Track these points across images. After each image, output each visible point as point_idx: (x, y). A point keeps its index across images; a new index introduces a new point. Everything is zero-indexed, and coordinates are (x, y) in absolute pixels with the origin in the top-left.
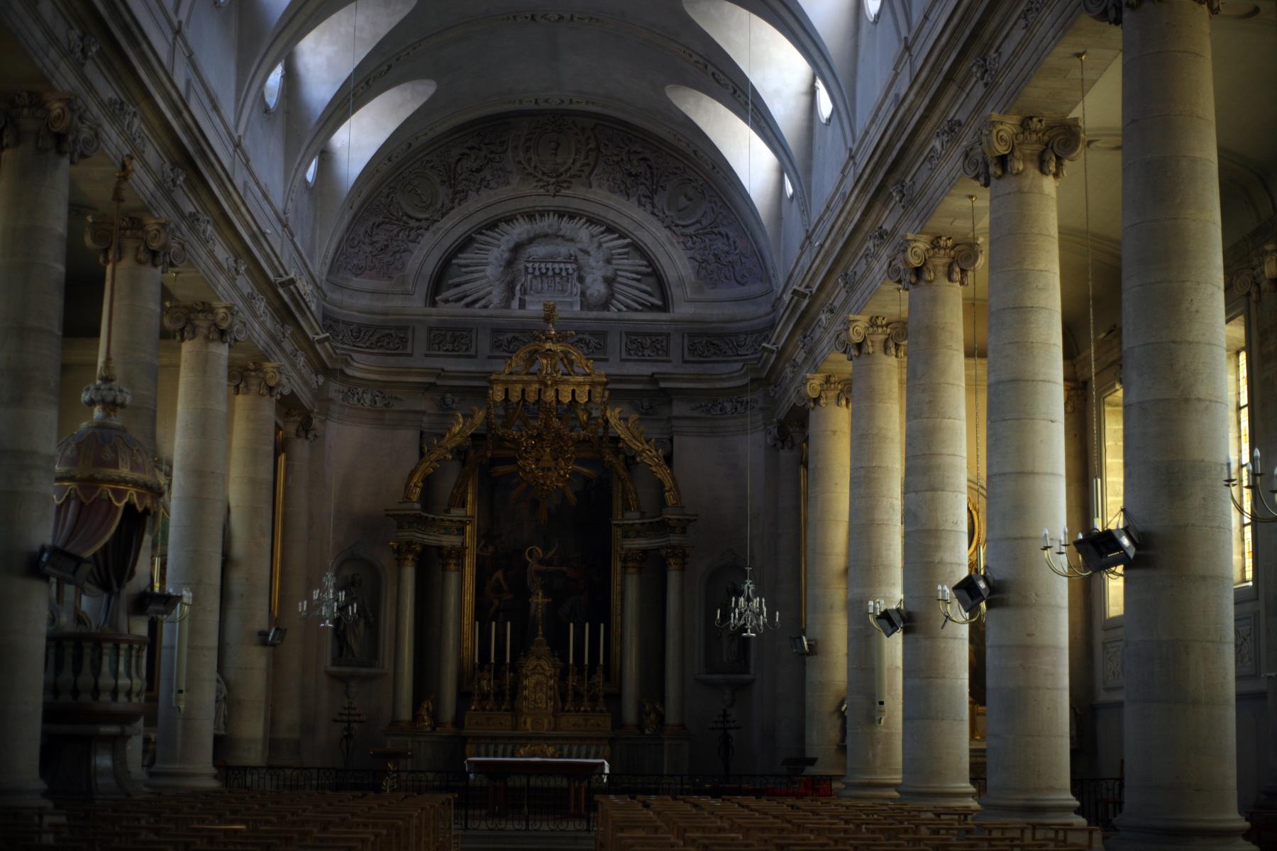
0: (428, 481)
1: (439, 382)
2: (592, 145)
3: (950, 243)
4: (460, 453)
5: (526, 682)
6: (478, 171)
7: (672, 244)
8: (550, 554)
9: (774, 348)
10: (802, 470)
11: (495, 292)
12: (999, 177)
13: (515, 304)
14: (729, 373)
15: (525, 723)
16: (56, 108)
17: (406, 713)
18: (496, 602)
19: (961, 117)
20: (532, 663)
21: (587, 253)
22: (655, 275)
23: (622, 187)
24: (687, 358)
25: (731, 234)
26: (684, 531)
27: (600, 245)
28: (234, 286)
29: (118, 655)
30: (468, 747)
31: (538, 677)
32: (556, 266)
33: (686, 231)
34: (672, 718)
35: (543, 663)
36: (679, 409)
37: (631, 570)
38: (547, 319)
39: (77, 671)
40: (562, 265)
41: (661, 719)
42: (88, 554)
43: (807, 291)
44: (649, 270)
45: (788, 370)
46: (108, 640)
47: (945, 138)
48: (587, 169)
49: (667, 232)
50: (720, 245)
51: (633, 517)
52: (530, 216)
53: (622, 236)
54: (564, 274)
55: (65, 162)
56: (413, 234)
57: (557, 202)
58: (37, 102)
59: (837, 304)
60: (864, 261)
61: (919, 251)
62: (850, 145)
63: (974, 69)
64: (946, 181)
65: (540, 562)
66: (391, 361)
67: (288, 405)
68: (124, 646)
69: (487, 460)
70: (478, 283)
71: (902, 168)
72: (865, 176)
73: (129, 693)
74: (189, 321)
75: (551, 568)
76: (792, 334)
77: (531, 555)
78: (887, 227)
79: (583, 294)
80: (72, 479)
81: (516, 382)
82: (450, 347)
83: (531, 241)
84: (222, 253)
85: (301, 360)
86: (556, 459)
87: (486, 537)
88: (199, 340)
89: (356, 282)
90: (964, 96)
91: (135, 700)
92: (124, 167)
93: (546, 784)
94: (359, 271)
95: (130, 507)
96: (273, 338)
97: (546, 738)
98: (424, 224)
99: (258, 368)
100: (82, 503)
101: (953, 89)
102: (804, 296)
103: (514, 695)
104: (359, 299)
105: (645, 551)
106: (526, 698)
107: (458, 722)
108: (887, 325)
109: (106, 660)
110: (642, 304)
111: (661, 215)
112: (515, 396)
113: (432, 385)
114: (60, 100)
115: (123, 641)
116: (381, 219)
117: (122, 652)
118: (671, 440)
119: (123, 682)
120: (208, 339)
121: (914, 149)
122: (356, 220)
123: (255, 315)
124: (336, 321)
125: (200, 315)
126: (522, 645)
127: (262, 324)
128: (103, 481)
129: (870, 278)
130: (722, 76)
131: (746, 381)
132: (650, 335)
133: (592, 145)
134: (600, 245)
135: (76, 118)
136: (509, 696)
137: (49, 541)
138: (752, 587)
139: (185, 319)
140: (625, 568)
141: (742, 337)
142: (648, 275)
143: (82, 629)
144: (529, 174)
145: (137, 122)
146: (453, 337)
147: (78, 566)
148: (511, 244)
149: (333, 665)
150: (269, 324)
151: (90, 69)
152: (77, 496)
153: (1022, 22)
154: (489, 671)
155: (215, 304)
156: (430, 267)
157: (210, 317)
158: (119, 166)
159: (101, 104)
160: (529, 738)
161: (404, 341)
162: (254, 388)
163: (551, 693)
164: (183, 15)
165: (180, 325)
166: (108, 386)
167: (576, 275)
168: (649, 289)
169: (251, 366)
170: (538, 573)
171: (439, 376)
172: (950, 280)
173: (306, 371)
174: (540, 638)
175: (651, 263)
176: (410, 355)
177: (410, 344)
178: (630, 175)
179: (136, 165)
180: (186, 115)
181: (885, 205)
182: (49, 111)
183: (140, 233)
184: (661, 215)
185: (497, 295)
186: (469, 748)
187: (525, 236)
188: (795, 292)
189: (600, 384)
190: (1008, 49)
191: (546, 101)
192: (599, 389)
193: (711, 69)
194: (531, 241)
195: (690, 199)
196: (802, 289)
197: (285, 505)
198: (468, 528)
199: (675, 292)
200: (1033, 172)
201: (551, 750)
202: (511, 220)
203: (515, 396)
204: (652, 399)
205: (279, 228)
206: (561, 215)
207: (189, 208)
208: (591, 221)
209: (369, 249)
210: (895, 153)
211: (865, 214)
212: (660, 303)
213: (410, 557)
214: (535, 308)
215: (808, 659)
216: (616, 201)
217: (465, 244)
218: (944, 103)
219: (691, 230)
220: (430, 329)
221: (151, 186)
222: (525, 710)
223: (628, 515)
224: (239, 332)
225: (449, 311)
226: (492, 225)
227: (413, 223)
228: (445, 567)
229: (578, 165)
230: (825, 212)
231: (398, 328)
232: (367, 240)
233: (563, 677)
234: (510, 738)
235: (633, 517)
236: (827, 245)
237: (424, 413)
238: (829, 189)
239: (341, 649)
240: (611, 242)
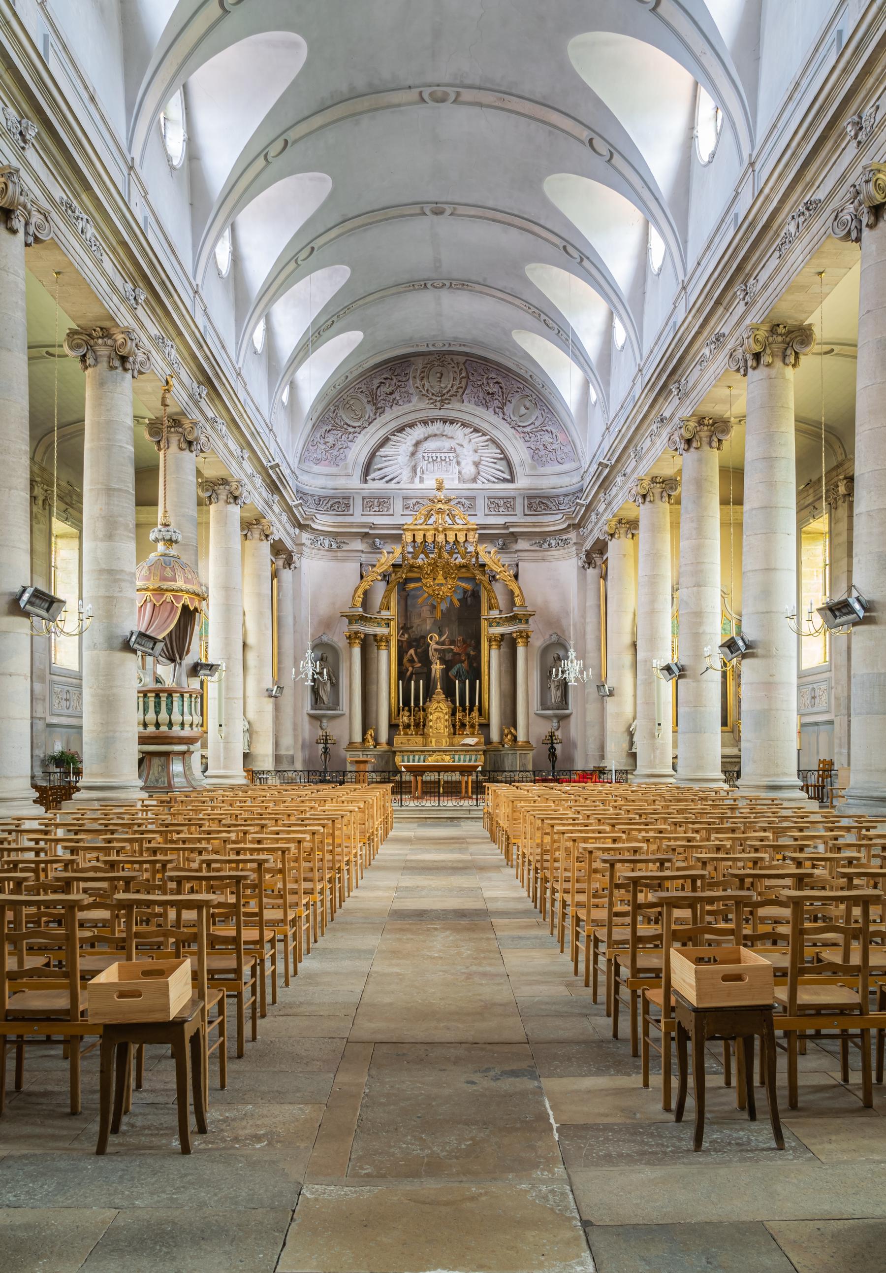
0: (366, 593)
1: (371, 532)
2: (464, 375)
3: (711, 422)
4: (385, 577)
5: (431, 717)
6: (391, 394)
7: (516, 438)
8: (443, 639)
9: (584, 503)
10: (602, 581)
11: (404, 473)
12: (754, 369)
13: (417, 480)
14: (554, 521)
16: (120, 338)
17: (358, 738)
18: (410, 669)
19: (726, 330)
20: (434, 705)
21: (462, 446)
22: (506, 459)
23: (484, 402)
24: (526, 512)
25: (554, 431)
26: (527, 621)
27: (470, 441)
28: (241, 467)
29: (183, 701)
31: (439, 713)
32: (442, 455)
33: (525, 430)
34: (521, 738)
35: (441, 705)
36: (522, 544)
37: (494, 647)
38: (439, 489)
39: (157, 713)
40: (446, 455)
41: (515, 739)
42: (160, 637)
43: (608, 463)
44: (502, 456)
45: (593, 517)
46: (176, 692)
47: (713, 346)
48: (461, 391)
49: (513, 430)
50: (547, 438)
51: (495, 614)
52: (425, 423)
53: (484, 435)
54: (447, 460)
55: (129, 375)
56: (351, 436)
57: (442, 413)
58: (106, 333)
59: (628, 471)
60: (649, 439)
61: (690, 428)
62: (638, 361)
63: (738, 293)
64: (713, 377)
65: (437, 643)
66: (340, 519)
67: (278, 549)
68: (186, 695)
69: (403, 580)
70: (393, 467)
71: (679, 372)
72: (653, 380)
73: (191, 725)
74: (214, 491)
75: (444, 647)
76: (597, 493)
77: (431, 638)
78: (667, 414)
79: (460, 473)
80: (147, 589)
81: (420, 530)
82: (377, 509)
83: (426, 439)
84: (233, 446)
85: (284, 517)
86: (446, 578)
87: (404, 628)
88: (222, 503)
89: (316, 469)
90: (728, 314)
91: (195, 729)
92: (167, 383)
93: (450, 778)
94: (318, 461)
95: (185, 608)
96: (267, 503)
97: (444, 751)
98: (358, 430)
99: (258, 522)
101: (721, 310)
102: (607, 466)
103: (424, 726)
104: (317, 479)
105: (502, 635)
106: (431, 727)
107: (390, 742)
108: (663, 482)
109: (175, 704)
110: (498, 479)
111: (508, 419)
112: (419, 539)
113: (367, 534)
114: (123, 333)
115: (187, 692)
116: (330, 427)
117: (185, 699)
118: (517, 565)
119: (188, 718)
121: (689, 358)
122: (315, 427)
123: (256, 489)
124: (305, 494)
125: (221, 487)
126: (429, 694)
127: (260, 494)
128: (167, 590)
129: (653, 450)
130: (551, 322)
131: (565, 526)
132: (503, 498)
133: (464, 375)
134: (470, 441)
135: (134, 345)
136: (420, 726)
137: (135, 629)
138: (574, 654)
139: (214, 488)
140: (490, 646)
141: (562, 498)
142: (501, 459)
143: (159, 686)
144: (423, 395)
145: (173, 352)
146: (379, 502)
147: (155, 644)
148: (414, 442)
149: (312, 709)
150: (265, 494)
151: (140, 312)
152: (151, 601)
153: (777, 254)
154: (410, 711)
155: (230, 479)
156: (363, 458)
158: (164, 383)
159: (150, 337)
160: (434, 751)
161: (348, 506)
162: (256, 536)
163: (446, 724)
164: (199, 280)
165: (209, 494)
166: (166, 528)
167: (455, 460)
168: (502, 468)
169: (255, 522)
170: (436, 650)
171: (371, 528)
172: (711, 447)
173: (288, 527)
174: (439, 690)
175: (502, 452)
176: (352, 515)
177: (351, 507)
178: (488, 393)
179: (174, 382)
180: (205, 348)
181: (666, 399)
182: (115, 341)
183: (180, 430)
184: (508, 419)
185: (406, 474)
187: (422, 437)
188: (600, 464)
189: (473, 530)
190: (764, 276)
191: (433, 345)
192: (472, 533)
193: (543, 317)
194: (426, 439)
195: (527, 409)
196: (605, 461)
197: (278, 611)
198: (392, 623)
199: (518, 470)
200: (779, 364)
201: (448, 758)
202: (413, 426)
203: (419, 539)
204: (506, 539)
205: (267, 431)
206: (445, 422)
207: (210, 415)
208: (464, 425)
209: (323, 447)
210: (675, 361)
211: (652, 406)
212: (509, 477)
213: (357, 641)
214: (430, 483)
215: (608, 699)
216: (480, 411)
217: (385, 441)
218: (712, 322)
219: (528, 429)
220: (364, 498)
221: (186, 398)
222: (431, 734)
223: (492, 612)
224: (246, 498)
225: (374, 486)
226: (401, 430)
227: (351, 430)
228: (378, 648)
229: (455, 388)
230: (620, 410)
231: (344, 498)
232: (322, 441)
233: (453, 714)
234: (422, 751)
235: (495, 614)
236: (623, 431)
237: (362, 551)
238: (622, 395)
239: (316, 700)
240: (477, 439)
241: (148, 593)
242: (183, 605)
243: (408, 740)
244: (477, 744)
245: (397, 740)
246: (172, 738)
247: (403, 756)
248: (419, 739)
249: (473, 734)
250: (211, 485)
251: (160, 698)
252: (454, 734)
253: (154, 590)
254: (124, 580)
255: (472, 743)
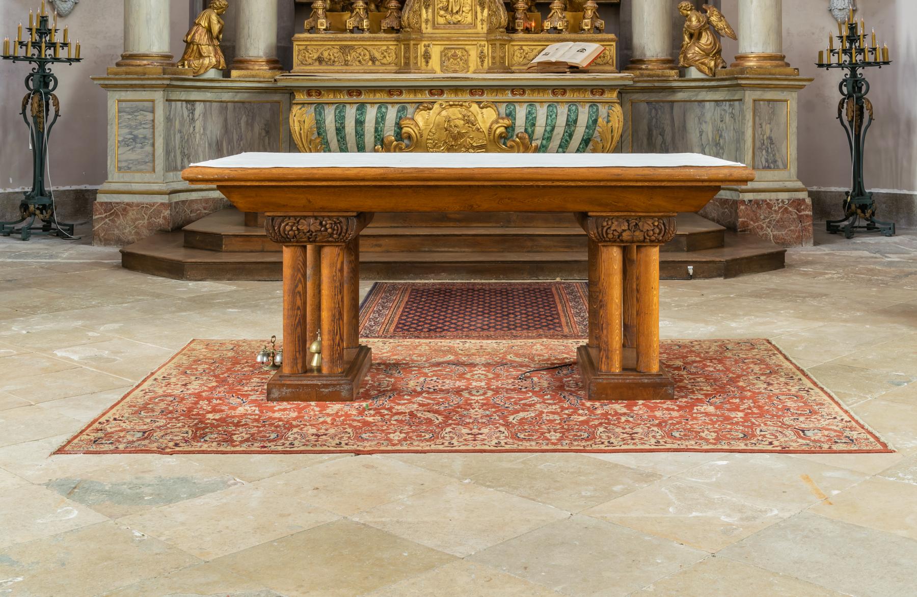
15: (427, 57)
30: (295, 109)
97: (474, 90)
107: (282, 59)
160: (437, 90)
186: (300, 118)
201: (487, 118)
222: (427, 29)
234: (391, 90)
243: (345, 50)
244: (596, 63)
245: (302, 42)
247: (319, 107)
248: (384, 46)
249: (576, 28)
252: (511, 29)
255: (581, 60)
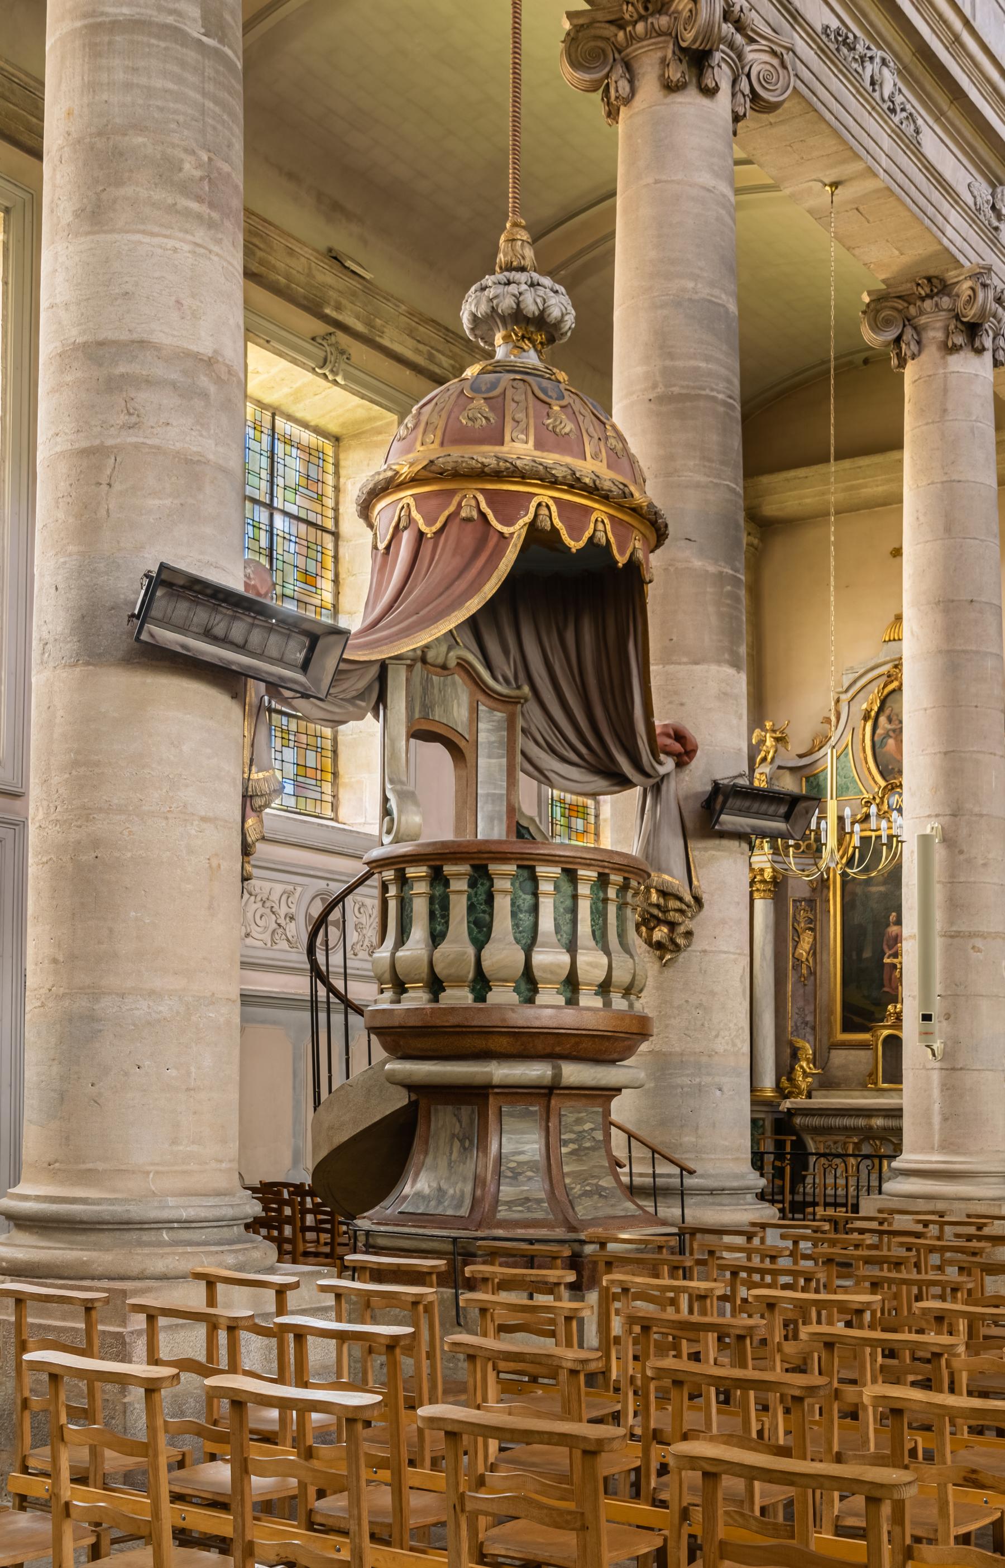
29: (535, 895)
46: (503, 857)
74: (908, 321)
88: (931, 353)
95: (540, 539)
100: (421, 534)
109: (502, 905)
115: (550, 860)
120: (950, 349)
125: (928, 304)
155: (951, 276)
157: (945, 302)
165: (891, 335)
241: (406, 495)
242: (532, 525)
246: (486, 1032)
250: (900, 304)
251: (447, 884)
253: (415, 480)
254: (149, 382)
